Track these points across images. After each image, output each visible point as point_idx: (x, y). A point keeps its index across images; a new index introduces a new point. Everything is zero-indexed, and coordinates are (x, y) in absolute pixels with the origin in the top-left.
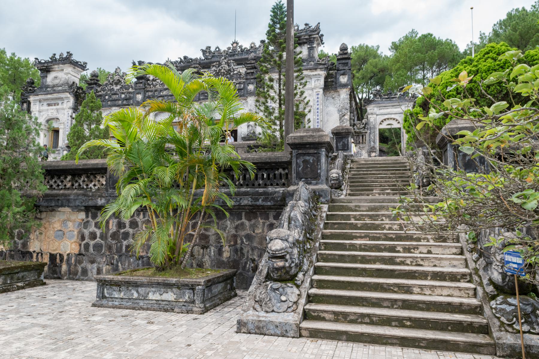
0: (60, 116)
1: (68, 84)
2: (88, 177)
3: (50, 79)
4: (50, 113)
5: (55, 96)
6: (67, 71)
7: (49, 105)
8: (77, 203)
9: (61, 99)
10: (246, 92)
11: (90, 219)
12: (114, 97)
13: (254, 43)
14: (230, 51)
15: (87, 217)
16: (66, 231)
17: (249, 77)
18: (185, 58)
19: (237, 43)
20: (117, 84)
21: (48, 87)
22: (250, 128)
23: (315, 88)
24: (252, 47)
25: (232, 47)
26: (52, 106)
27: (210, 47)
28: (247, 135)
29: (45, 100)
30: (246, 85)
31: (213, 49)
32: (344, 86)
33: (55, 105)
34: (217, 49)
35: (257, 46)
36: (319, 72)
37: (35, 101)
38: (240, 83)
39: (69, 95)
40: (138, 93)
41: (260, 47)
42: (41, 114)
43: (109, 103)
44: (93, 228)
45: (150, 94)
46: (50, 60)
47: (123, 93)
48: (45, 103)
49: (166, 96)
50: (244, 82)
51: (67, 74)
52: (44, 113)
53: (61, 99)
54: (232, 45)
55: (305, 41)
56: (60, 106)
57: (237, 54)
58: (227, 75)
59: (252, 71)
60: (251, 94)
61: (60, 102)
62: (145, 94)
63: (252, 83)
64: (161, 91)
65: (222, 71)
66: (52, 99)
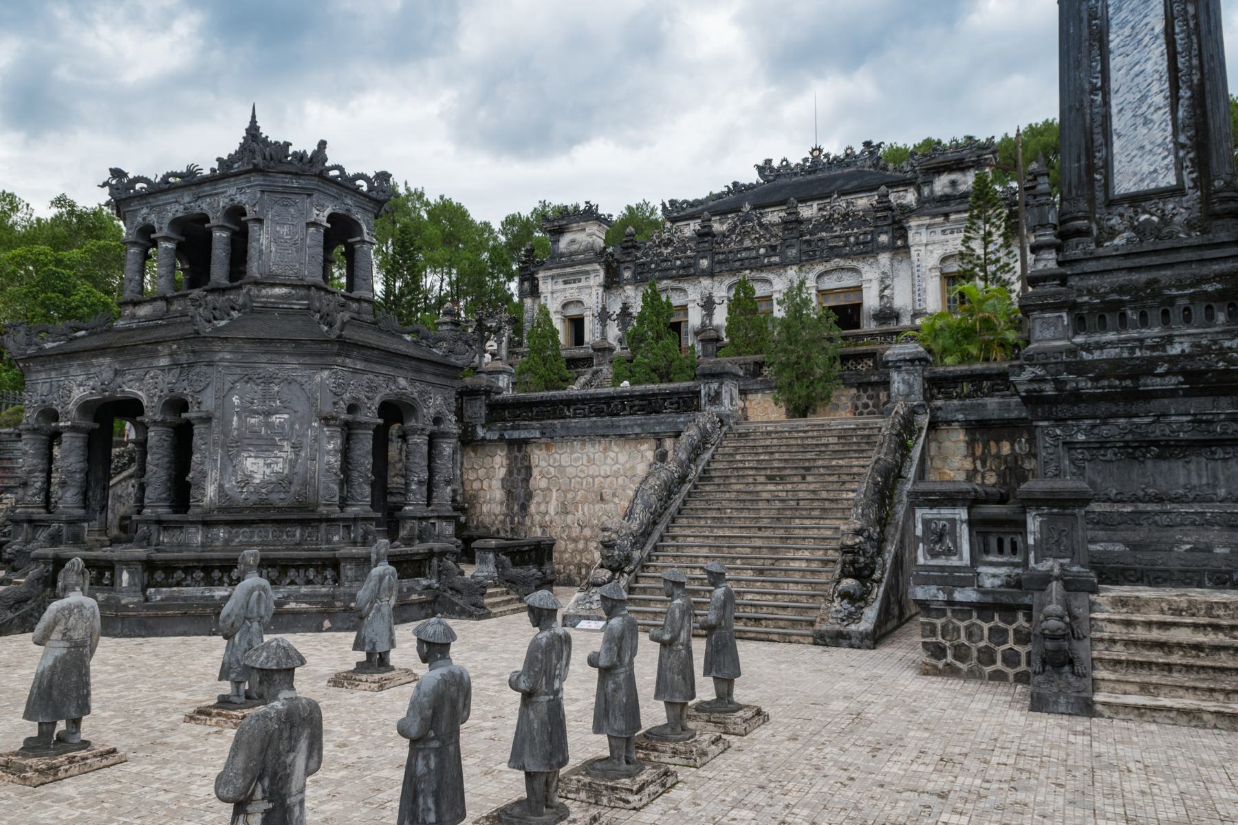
0: (584, 297)
1: (592, 249)
2: (856, 361)
3: (564, 243)
4: (568, 295)
5: (577, 268)
7: (565, 282)
8: (853, 381)
9: (587, 273)
10: (875, 246)
11: (861, 393)
12: (664, 265)
13: (851, 148)
14: (808, 164)
15: (859, 391)
16: (840, 404)
17: (879, 223)
18: (735, 184)
19: (820, 150)
20: (666, 245)
21: (562, 255)
22: (885, 300)
24: (847, 155)
25: (810, 156)
27: (770, 161)
28: (880, 311)
29: (560, 276)
30: (876, 236)
31: (776, 164)
34: (784, 163)
35: (858, 152)
38: (865, 233)
39: (598, 267)
40: (702, 258)
41: (862, 153)
42: (555, 296)
43: (657, 274)
44: (865, 400)
45: (721, 257)
47: (678, 259)
48: (560, 280)
49: (746, 259)
50: (872, 231)
51: (591, 235)
52: (558, 294)
54: (811, 153)
55: (970, 164)
56: (583, 283)
57: (821, 169)
58: (843, 221)
59: (885, 214)
60: (884, 248)
61: (583, 278)
62: (713, 258)
63: (886, 233)
64: (738, 252)
65: (836, 216)
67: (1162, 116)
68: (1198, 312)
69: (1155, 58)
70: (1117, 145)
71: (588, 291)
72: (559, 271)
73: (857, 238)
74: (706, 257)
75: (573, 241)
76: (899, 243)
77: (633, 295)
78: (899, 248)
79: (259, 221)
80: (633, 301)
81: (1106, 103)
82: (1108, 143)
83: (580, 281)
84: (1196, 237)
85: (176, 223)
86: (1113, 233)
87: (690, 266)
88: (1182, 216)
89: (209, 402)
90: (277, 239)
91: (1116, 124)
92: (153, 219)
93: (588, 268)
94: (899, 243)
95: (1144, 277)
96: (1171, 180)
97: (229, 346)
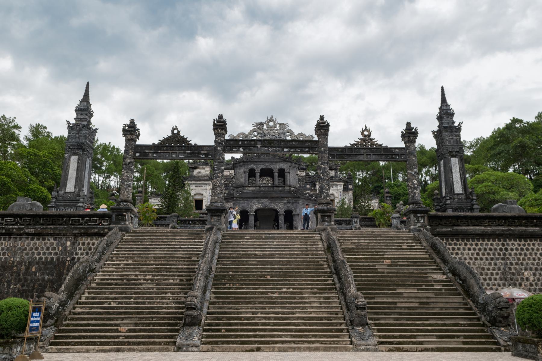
0: (204, 193)
3: (196, 172)
5: (202, 182)
7: (196, 187)
9: (206, 184)
21: (195, 177)
23: (339, 190)
32: (351, 190)
33: (200, 187)
36: (341, 183)
38: (303, 184)
43: (232, 188)
48: (194, 186)
51: (207, 171)
56: (204, 188)
61: (204, 186)
63: (309, 185)
66: (199, 184)
67: (460, 183)
68: (467, 211)
69: (458, 175)
70: (455, 186)
71: (206, 191)
72: (195, 182)
73: (300, 185)
75: (200, 172)
76: (313, 188)
78: (313, 190)
79: (289, 173)
81: (453, 180)
82: (453, 186)
84: (465, 201)
85: (262, 170)
86: (455, 199)
88: (463, 198)
89: (298, 211)
90: (292, 177)
91: (454, 183)
92: (255, 167)
93: (207, 182)
94: (313, 188)
95: (460, 205)
96: (461, 192)
97: (302, 200)
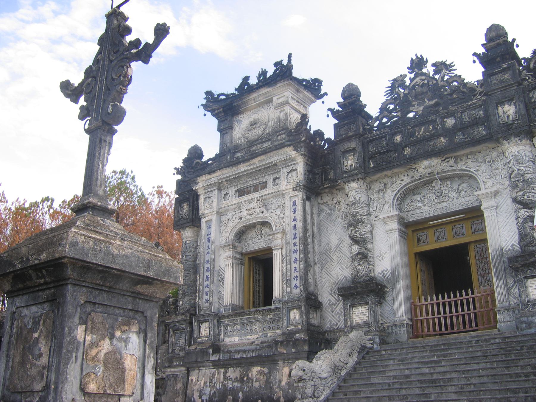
0: (271, 217)
5: (257, 162)
6: (280, 101)
7: (241, 193)
9: (273, 168)
26: (249, 193)
33: (256, 190)
37: (208, 188)
39: (293, 153)
40: (501, 103)
42: (224, 218)
46: (237, 93)
48: (232, 191)
53: (273, 168)
56: (270, 189)
61: (269, 179)
66: (250, 174)
71: (277, 201)
74: (510, 100)
75: (254, 124)
77: (364, 198)
80: (363, 211)
83: (264, 185)
87: (475, 123)
93: (275, 158)
